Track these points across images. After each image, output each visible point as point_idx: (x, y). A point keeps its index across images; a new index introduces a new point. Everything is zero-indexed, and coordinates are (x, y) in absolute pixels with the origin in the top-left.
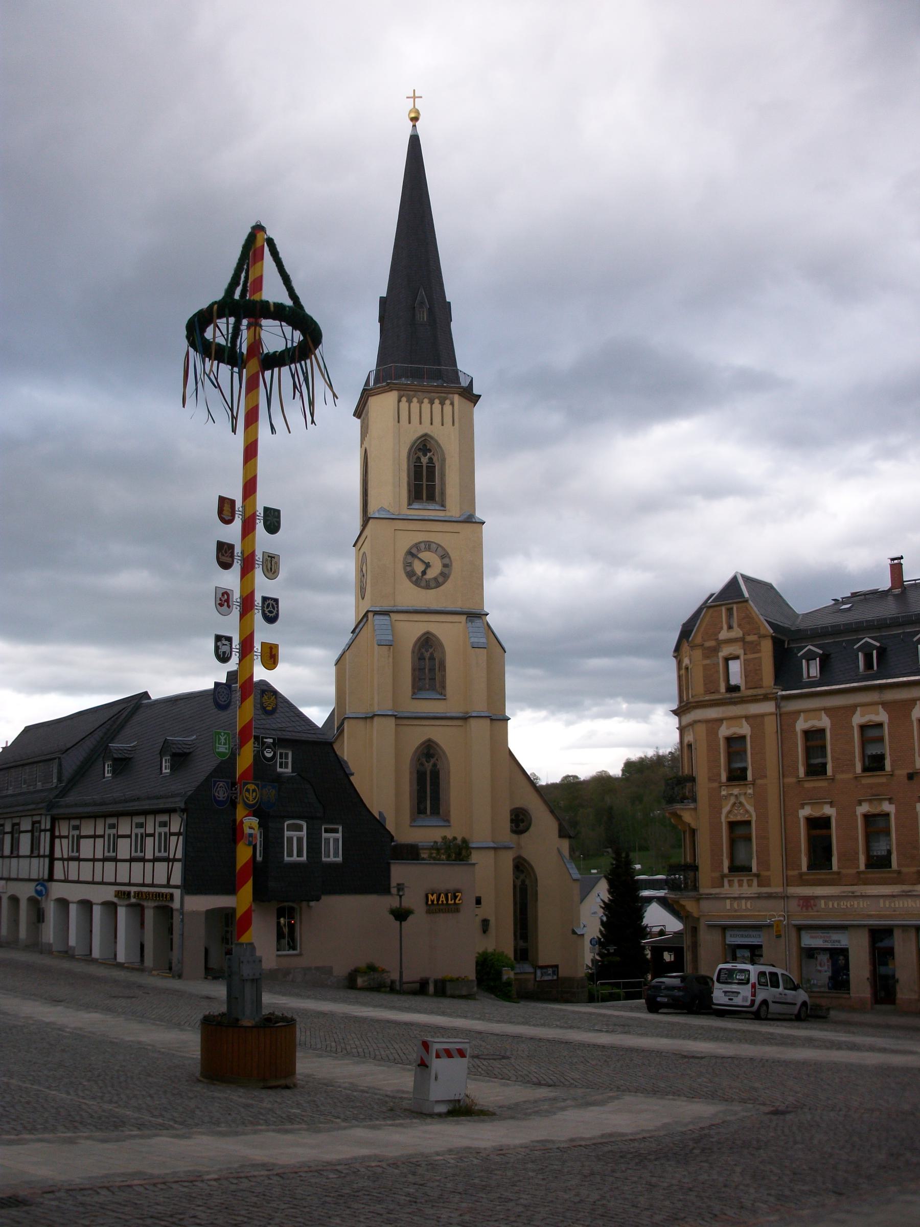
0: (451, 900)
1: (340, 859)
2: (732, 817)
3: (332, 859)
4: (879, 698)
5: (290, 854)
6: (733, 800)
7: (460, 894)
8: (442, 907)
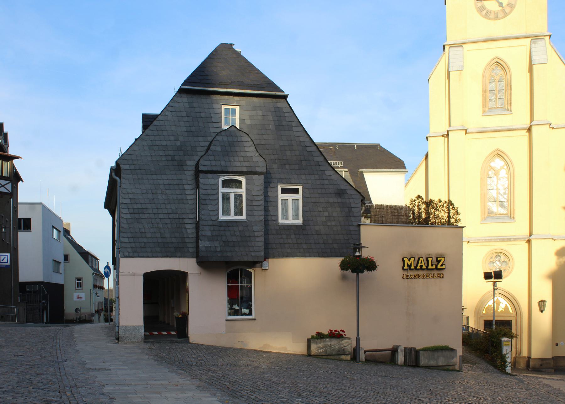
0: (432, 265)
1: (300, 221)
3: (290, 221)
5: (226, 212)
7: (443, 259)
8: (421, 272)
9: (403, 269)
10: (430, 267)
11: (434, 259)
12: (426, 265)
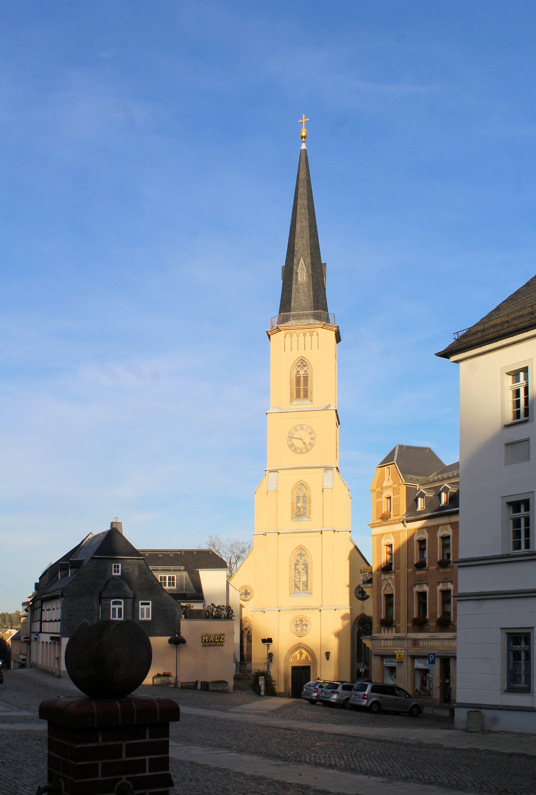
0: (217, 640)
1: (150, 618)
2: (386, 592)
3: (145, 618)
4: (449, 520)
5: (114, 616)
6: (386, 582)
7: (223, 637)
8: (212, 643)
9: (203, 642)
10: (216, 641)
11: (219, 636)
12: (214, 640)
